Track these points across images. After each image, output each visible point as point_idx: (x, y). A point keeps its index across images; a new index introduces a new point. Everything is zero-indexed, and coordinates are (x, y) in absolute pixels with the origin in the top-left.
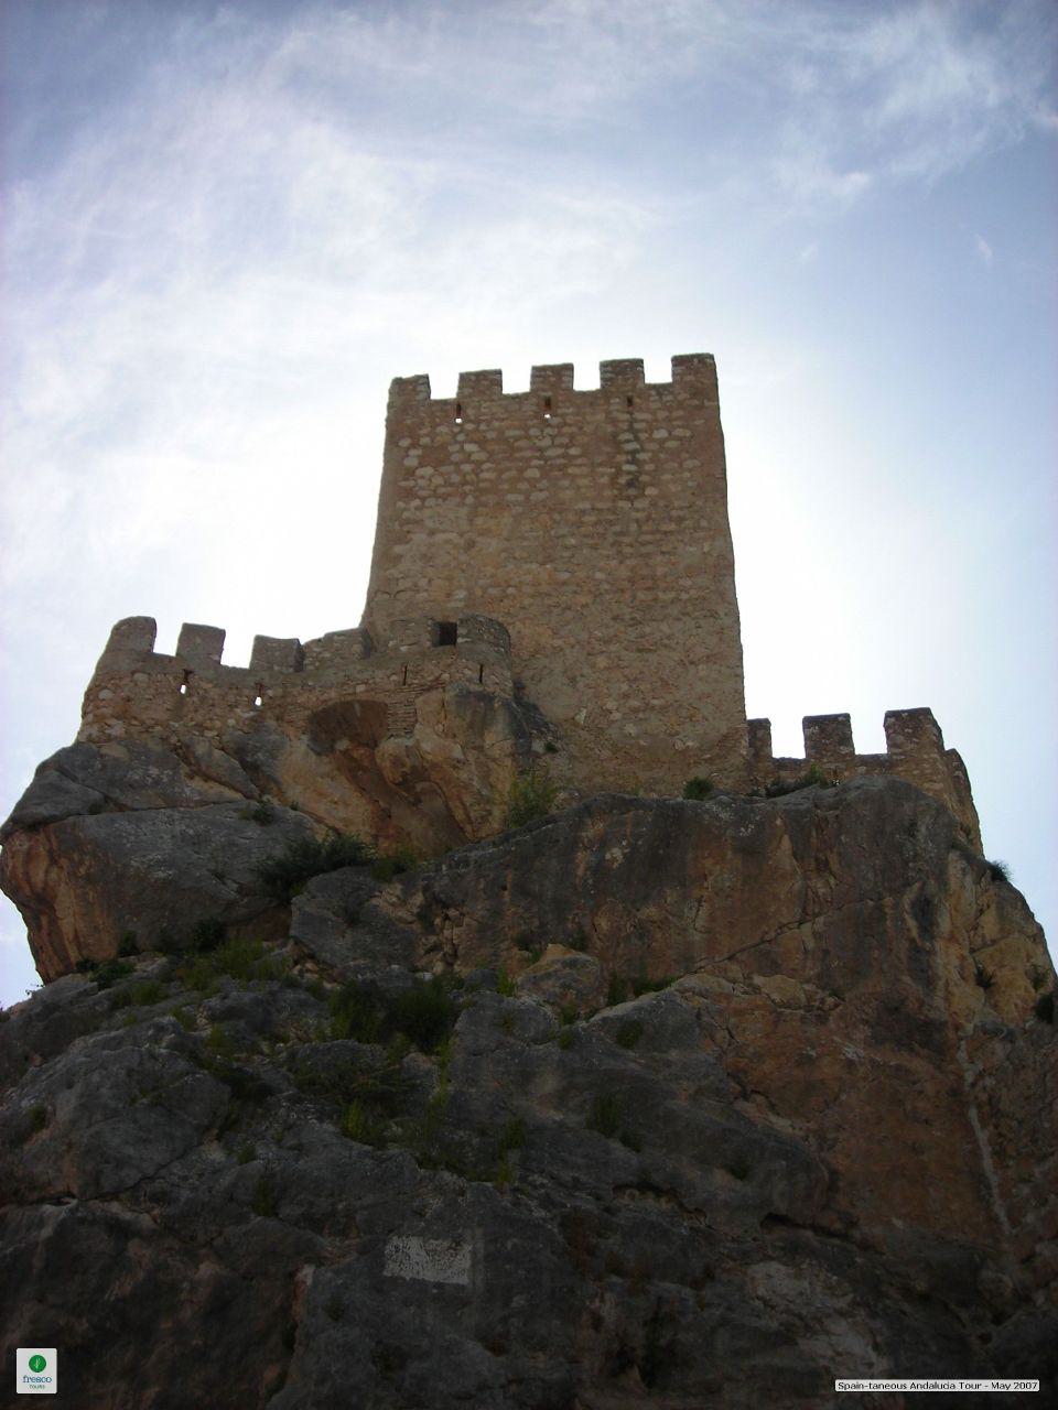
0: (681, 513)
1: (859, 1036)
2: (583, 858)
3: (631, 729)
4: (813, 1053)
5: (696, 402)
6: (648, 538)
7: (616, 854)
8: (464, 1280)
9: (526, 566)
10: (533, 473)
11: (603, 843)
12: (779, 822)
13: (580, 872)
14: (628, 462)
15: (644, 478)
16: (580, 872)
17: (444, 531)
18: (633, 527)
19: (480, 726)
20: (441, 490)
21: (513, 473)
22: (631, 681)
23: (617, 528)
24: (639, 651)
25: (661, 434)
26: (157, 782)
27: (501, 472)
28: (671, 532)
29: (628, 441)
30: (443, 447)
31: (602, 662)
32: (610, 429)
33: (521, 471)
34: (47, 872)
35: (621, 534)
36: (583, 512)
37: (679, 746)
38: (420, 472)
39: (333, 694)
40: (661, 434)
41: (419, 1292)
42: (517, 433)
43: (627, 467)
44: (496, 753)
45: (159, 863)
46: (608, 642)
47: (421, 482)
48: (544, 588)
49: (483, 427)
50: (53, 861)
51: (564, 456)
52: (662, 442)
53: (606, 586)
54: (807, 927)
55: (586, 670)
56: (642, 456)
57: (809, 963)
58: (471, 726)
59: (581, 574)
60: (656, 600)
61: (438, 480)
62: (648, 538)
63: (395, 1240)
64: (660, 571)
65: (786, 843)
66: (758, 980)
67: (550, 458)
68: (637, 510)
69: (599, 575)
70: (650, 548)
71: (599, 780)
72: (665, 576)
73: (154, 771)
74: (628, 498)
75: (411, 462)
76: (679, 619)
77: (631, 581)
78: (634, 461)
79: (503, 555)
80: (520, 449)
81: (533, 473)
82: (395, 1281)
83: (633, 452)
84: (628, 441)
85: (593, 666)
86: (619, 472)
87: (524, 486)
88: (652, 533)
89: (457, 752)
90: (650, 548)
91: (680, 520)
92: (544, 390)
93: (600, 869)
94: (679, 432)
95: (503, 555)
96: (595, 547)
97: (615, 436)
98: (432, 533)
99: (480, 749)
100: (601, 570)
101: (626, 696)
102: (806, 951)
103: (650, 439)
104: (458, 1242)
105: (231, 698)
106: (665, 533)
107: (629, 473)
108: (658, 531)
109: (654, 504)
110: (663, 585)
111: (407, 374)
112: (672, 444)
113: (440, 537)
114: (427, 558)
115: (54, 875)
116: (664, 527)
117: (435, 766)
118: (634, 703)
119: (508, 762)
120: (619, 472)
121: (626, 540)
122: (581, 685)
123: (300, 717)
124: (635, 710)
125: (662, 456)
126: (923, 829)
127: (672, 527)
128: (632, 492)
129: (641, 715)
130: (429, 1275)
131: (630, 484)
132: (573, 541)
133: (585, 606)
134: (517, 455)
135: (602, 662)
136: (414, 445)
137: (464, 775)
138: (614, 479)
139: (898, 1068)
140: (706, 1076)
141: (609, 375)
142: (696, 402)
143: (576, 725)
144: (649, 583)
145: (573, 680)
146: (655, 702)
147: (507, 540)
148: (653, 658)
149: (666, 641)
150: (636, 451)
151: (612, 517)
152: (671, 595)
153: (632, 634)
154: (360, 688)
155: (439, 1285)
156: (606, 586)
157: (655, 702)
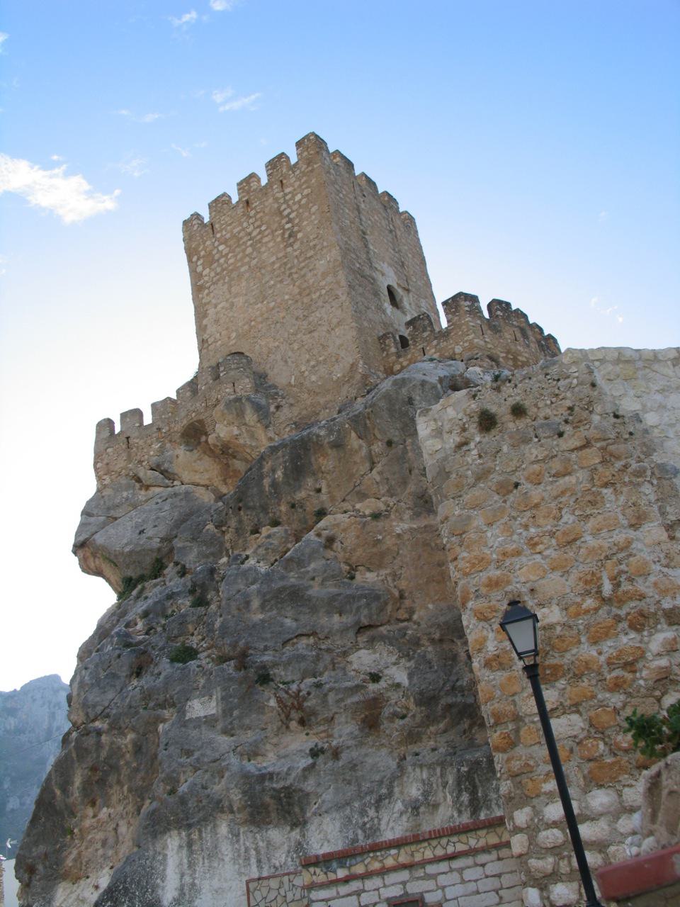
0: (314, 243)
1: (406, 517)
2: (266, 482)
3: (314, 378)
4: (380, 537)
5: (310, 168)
6: (303, 264)
8: (214, 712)
9: (256, 307)
10: (249, 250)
11: (274, 471)
12: (347, 426)
13: (267, 489)
14: (287, 223)
16: (267, 489)
17: (219, 304)
18: (296, 261)
19: (241, 414)
21: (241, 254)
22: (309, 351)
23: (289, 266)
24: (310, 333)
25: (298, 197)
26: (127, 499)
28: (312, 257)
29: (285, 209)
31: (296, 346)
32: (276, 206)
33: (244, 251)
34: (94, 562)
35: (290, 269)
36: (273, 263)
37: (335, 378)
39: (185, 422)
40: (298, 197)
41: (198, 723)
42: (238, 229)
44: (252, 423)
45: (126, 544)
46: (295, 334)
47: (206, 279)
49: (224, 233)
50: (95, 557)
51: (259, 233)
53: (290, 302)
54: (374, 471)
55: (290, 354)
57: (381, 487)
58: (238, 415)
59: (279, 301)
61: (213, 274)
62: (303, 264)
63: (189, 703)
64: (311, 281)
65: (353, 434)
66: (358, 506)
67: (255, 237)
72: (313, 284)
73: (125, 494)
74: (291, 245)
75: (199, 269)
76: (323, 307)
77: (300, 294)
78: (290, 221)
79: (246, 305)
81: (249, 250)
82: (190, 720)
84: (285, 209)
86: (285, 231)
87: (247, 259)
88: (304, 261)
89: (236, 432)
90: (305, 270)
92: (244, 197)
93: (274, 484)
95: (246, 305)
96: (281, 282)
97: (279, 208)
98: (216, 306)
99: (245, 424)
100: (287, 294)
101: (308, 361)
102: (377, 483)
103: (294, 204)
104: (211, 696)
105: (149, 442)
106: (310, 258)
107: (288, 229)
108: (306, 258)
110: (313, 290)
111: (187, 216)
113: (220, 306)
115: (97, 562)
116: (308, 255)
117: (229, 442)
118: (312, 363)
119: (259, 425)
120: (285, 231)
122: (290, 363)
123: (177, 437)
124: (314, 367)
125: (301, 211)
126: (418, 398)
127: (312, 253)
128: (292, 240)
129: (316, 368)
131: (290, 236)
132: (272, 282)
133: (284, 318)
134: (241, 242)
135: (296, 346)
137: (241, 441)
139: (425, 527)
140: (325, 571)
141: (270, 172)
142: (310, 168)
143: (292, 386)
145: (286, 362)
146: (321, 359)
147: (246, 295)
148: (315, 334)
149: (320, 322)
150: (289, 214)
152: (318, 294)
153: (305, 323)
154: (194, 414)
155: (205, 717)
156: (290, 302)
157: (321, 359)
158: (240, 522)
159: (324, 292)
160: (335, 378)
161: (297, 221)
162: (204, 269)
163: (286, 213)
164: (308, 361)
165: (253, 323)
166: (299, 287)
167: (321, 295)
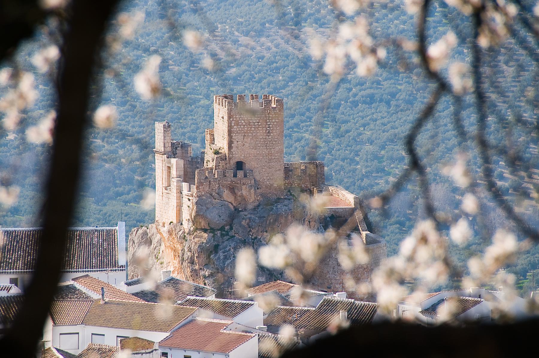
3: (268, 183)
5: (280, 113)
6: (271, 145)
7: (272, 220)
10: (253, 129)
15: (271, 131)
19: (250, 190)
20: (238, 132)
23: (266, 143)
27: (248, 128)
30: (238, 121)
33: (251, 128)
35: (266, 144)
38: (234, 127)
42: (250, 119)
43: (268, 129)
48: (255, 155)
51: (258, 125)
52: (274, 122)
56: (271, 126)
60: (272, 158)
61: (238, 129)
62: (271, 145)
68: (269, 139)
69: (264, 153)
70: (270, 147)
71: (263, 192)
80: (251, 123)
81: (253, 129)
83: (269, 125)
85: (263, 171)
88: (272, 144)
90: (270, 147)
91: (276, 141)
93: (270, 223)
94: (276, 120)
96: (263, 146)
98: (237, 142)
101: (267, 177)
109: (272, 137)
112: (275, 123)
114: (237, 147)
118: (268, 178)
121: (267, 145)
124: (268, 179)
127: (275, 143)
128: (269, 134)
130: (261, 281)
131: (268, 132)
135: (264, 170)
136: (233, 120)
138: (266, 130)
142: (280, 113)
144: (271, 155)
151: (265, 140)
152: (274, 157)
158: (259, 229)
159: (276, 158)
160: (274, 186)
161: (272, 129)
162: (234, 126)
163: (269, 123)
164: (267, 177)
165: (250, 155)
166: (268, 151)
167: (275, 158)
